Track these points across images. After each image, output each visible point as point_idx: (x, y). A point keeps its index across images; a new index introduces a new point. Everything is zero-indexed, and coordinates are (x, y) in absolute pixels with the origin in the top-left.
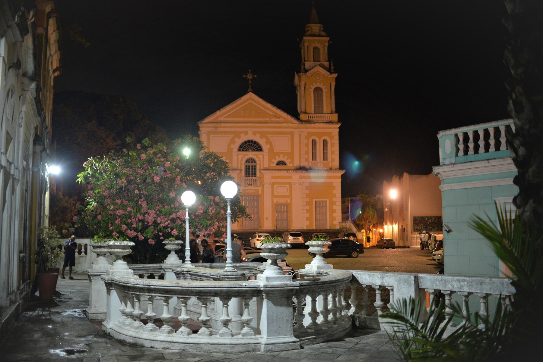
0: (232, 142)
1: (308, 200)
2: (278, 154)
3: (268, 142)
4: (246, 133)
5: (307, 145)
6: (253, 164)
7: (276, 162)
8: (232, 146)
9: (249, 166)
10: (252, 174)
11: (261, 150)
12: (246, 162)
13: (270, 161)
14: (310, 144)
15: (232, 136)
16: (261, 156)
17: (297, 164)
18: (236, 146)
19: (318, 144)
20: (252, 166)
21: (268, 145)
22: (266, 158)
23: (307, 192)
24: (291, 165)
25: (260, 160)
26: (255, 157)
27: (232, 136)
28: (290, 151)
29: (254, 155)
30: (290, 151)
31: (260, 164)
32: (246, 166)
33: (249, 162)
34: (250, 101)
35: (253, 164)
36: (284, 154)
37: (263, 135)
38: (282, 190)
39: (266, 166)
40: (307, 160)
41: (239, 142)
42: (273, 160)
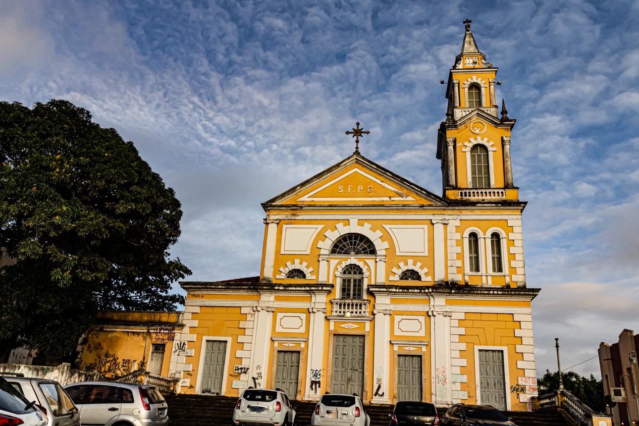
0: (322, 236)
1: (463, 346)
2: (405, 258)
3: (386, 237)
4: (347, 222)
5: (460, 243)
6: (358, 277)
7: (399, 272)
8: (320, 244)
9: (349, 281)
10: (354, 295)
11: (373, 252)
12: (345, 273)
13: (389, 272)
14: (466, 242)
15: (320, 227)
16: (371, 263)
17: (440, 276)
18: (326, 246)
19: (481, 242)
20: (355, 280)
21: (386, 243)
22: (382, 266)
23: (462, 331)
24: (429, 279)
25: (369, 269)
26: (361, 264)
27: (320, 227)
28: (426, 254)
29: (360, 260)
30: (426, 254)
31: (369, 277)
32: (344, 280)
33: (350, 273)
34: (356, 170)
35: (358, 277)
36: (416, 259)
37: (376, 225)
38: (412, 327)
39: (381, 280)
40: (460, 269)
41: (333, 236)
42: (395, 270)
